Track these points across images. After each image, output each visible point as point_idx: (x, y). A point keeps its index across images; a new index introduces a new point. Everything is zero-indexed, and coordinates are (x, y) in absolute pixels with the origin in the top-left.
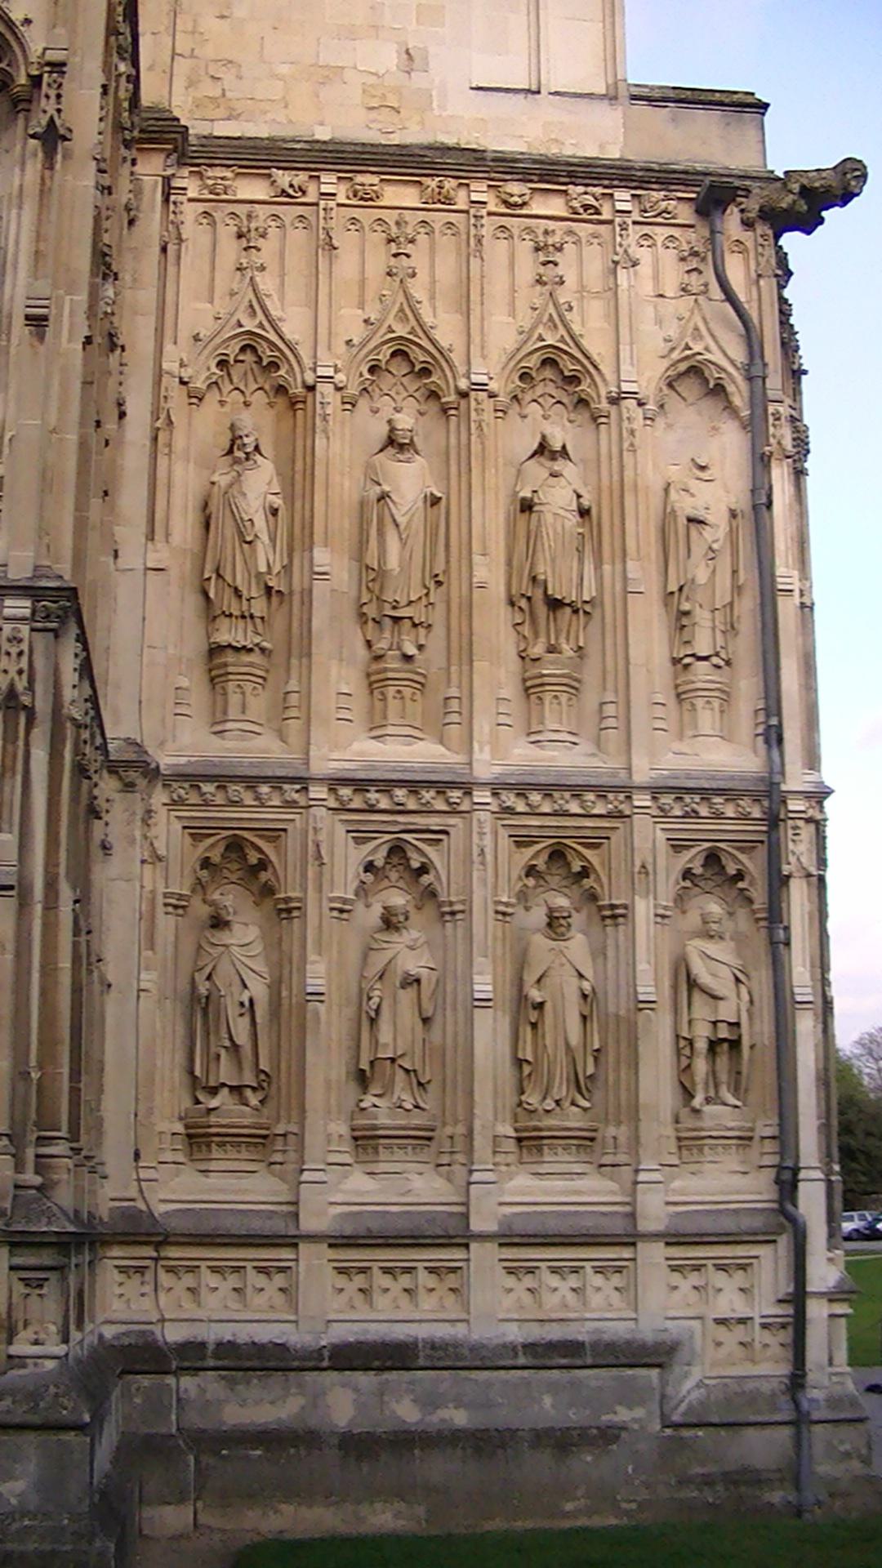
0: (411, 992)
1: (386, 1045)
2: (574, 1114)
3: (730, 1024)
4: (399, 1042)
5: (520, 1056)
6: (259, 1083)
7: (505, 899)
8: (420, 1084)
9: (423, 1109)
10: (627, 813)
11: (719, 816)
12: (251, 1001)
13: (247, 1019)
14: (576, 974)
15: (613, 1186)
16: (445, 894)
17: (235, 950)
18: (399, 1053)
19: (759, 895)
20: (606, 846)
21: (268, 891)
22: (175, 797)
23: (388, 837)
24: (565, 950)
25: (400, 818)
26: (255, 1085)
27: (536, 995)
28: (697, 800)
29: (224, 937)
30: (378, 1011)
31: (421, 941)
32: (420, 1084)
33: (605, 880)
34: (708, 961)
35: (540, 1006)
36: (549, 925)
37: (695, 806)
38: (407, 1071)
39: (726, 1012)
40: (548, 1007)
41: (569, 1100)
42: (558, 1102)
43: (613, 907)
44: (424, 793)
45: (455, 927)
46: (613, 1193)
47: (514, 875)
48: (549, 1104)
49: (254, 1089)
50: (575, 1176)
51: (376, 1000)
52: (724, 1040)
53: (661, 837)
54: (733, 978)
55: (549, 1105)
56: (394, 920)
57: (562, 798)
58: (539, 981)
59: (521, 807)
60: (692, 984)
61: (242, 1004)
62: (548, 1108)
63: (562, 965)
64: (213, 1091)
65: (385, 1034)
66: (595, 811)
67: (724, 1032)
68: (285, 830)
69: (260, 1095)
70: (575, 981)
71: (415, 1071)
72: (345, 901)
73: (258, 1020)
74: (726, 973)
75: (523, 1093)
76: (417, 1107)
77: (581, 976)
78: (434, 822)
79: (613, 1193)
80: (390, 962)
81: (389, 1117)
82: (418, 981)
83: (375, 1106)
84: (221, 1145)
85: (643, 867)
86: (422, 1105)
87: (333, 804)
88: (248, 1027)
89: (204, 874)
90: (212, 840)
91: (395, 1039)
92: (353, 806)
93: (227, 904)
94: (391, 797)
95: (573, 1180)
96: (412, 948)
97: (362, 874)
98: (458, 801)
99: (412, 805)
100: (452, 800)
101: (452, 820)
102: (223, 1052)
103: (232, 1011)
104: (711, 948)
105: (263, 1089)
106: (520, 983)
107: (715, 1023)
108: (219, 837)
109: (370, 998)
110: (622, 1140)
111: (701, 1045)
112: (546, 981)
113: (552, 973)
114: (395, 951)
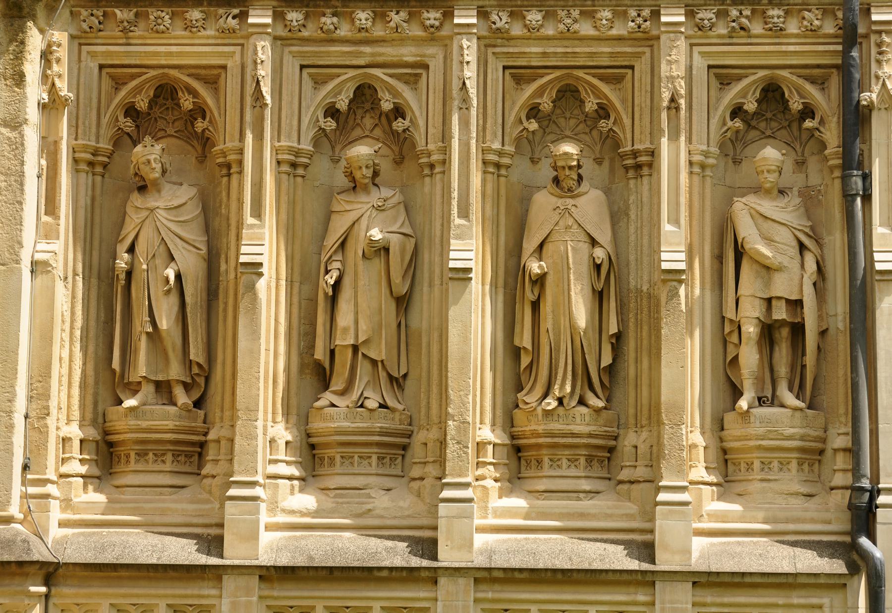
0: (378, 264)
1: (345, 330)
2: (583, 416)
3: (788, 302)
4: (363, 326)
5: (517, 342)
6: (192, 378)
7: (497, 145)
8: (391, 378)
9: (393, 410)
10: (655, 32)
11: (778, 32)
12: (178, 277)
13: (174, 299)
14: (587, 239)
15: (631, 508)
16: (424, 143)
17: (161, 214)
18: (361, 339)
19: (832, 136)
20: (629, 76)
21: (205, 142)
22: (85, 26)
23: (351, 73)
24: (573, 209)
25: (367, 49)
26: (189, 380)
27: (535, 267)
28: (747, 12)
29: (152, 201)
30: (337, 286)
31: (395, 200)
32: (391, 378)
33: (627, 121)
34: (760, 220)
35: (540, 281)
36: (556, 181)
37: (744, 20)
38: (374, 362)
39: (782, 286)
40: (550, 282)
41: (577, 398)
42: (560, 401)
43: (635, 154)
44: (392, 14)
45: (432, 185)
46: (630, 517)
47: (511, 118)
48: (551, 403)
49: (187, 387)
50: (581, 495)
51: (335, 274)
52: (783, 323)
53: (700, 64)
54: (795, 243)
55: (549, 404)
56: (358, 175)
57: (569, 15)
58: (541, 246)
59: (517, 30)
60: (739, 254)
61: (167, 280)
62: (550, 408)
63: (568, 227)
64: (134, 389)
65: (345, 317)
66: (614, 32)
67: (780, 313)
68: (224, 67)
69: (196, 395)
70: (585, 247)
71: (382, 361)
72: (297, 153)
73: (188, 299)
74: (785, 237)
75: (520, 388)
76: (381, 406)
77: (594, 242)
78: (408, 53)
79: (630, 517)
80: (354, 223)
81: (346, 418)
82: (387, 250)
83: (333, 405)
84: (142, 454)
85: (673, 100)
86: (390, 402)
87: (281, 32)
88: (176, 309)
89: (128, 125)
90: (133, 83)
91: (356, 322)
92: (305, 33)
93: (152, 157)
94: (353, 21)
95: (579, 499)
96: (379, 209)
97: (321, 119)
98: (437, 23)
99: (378, 32)
100: (428, 23)
101: (430, 51)
102: (144, 338)
103: (157, 290)
104: (767, 206)
105: (199, 385)
106: (516, 250)
107: (769, 301)
108: (144, 77)
109: (327, 272)
110: (642, 448)
111: (751, 330)
112: (549, 248)
113: (553, 238)
114: (360, 212)
